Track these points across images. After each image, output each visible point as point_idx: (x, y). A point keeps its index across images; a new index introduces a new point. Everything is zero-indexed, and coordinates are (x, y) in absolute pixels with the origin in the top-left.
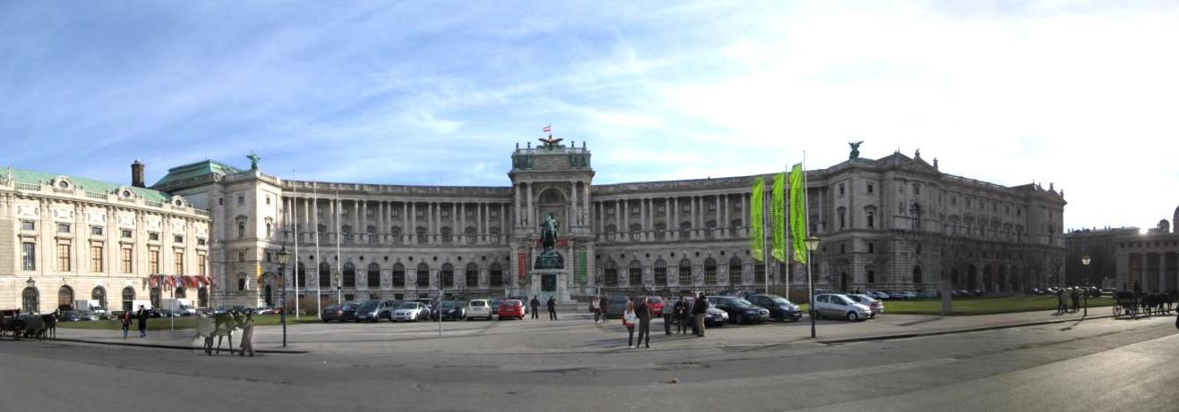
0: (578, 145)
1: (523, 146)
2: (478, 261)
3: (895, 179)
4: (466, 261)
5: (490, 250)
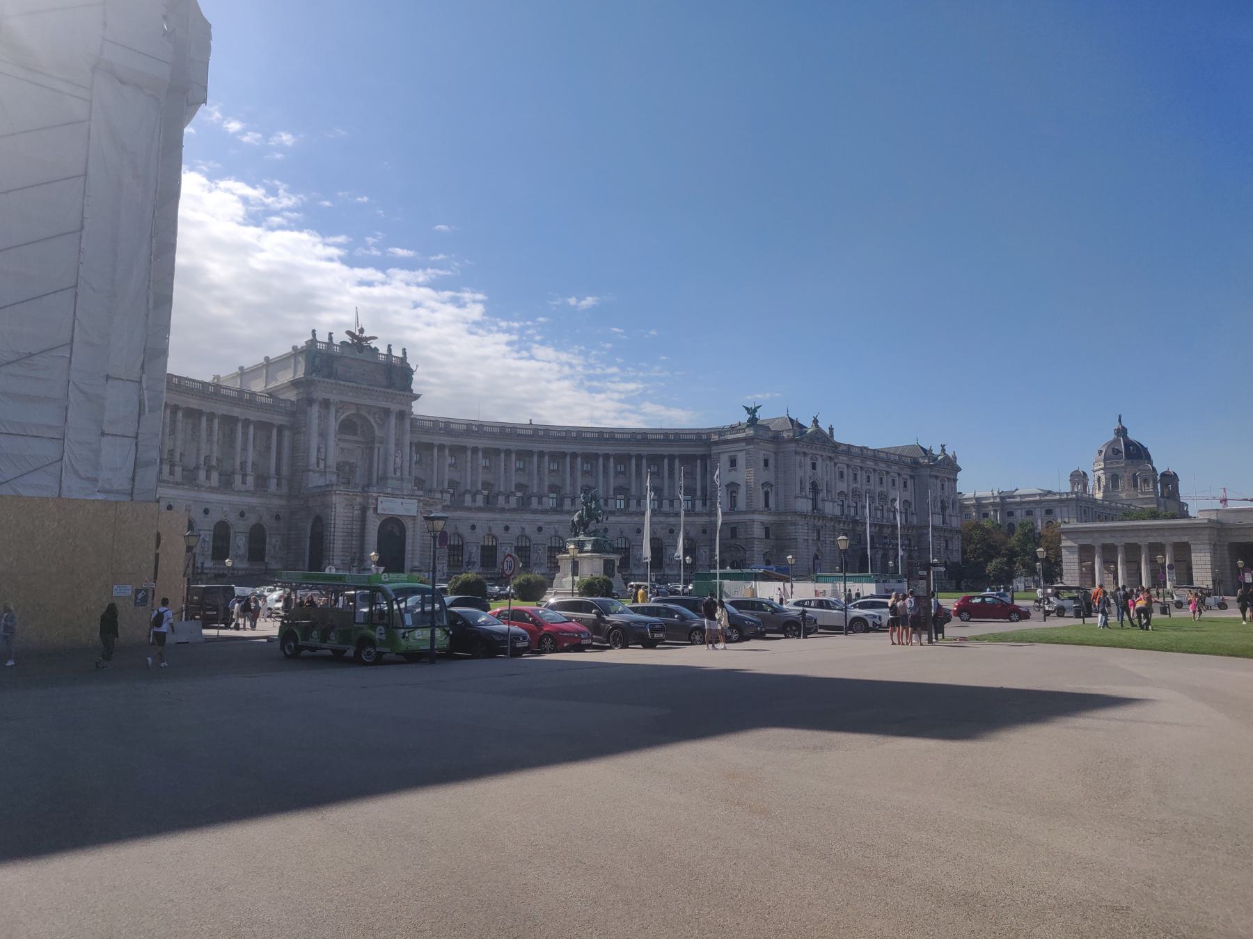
0: (397, 353)
1: (322, 337)
2: (232, 518)
3: (796, 453)
4: (216, 517)
5: (254, 501)
